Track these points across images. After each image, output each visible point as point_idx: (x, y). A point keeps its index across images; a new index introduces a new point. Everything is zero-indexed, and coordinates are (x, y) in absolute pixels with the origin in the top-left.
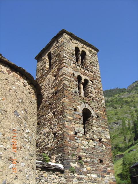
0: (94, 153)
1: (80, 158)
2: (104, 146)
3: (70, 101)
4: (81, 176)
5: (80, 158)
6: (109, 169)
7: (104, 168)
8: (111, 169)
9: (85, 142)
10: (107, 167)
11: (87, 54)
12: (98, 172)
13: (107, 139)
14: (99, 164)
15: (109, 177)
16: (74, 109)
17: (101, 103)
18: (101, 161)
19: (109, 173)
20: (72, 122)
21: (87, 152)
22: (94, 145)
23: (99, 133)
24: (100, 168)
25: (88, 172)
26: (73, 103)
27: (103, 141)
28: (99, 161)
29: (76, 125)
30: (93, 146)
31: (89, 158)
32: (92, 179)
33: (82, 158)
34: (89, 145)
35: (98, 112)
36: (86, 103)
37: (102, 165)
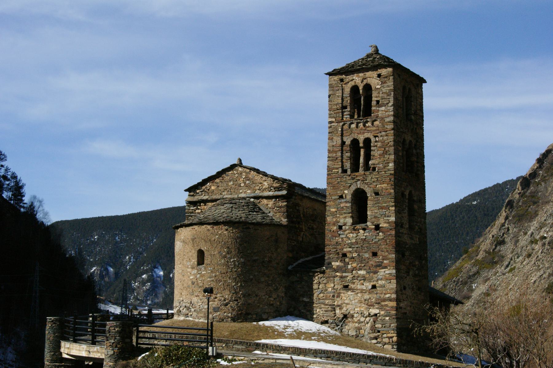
0: (363, 246)
1: (345, 255)
2: (381, 234)
3: (334, 188)
4: (344, 274)
5: (345, 255)
6: (385, 262)
7: (377, 262)
8: (390, 262)
9: (351, 235)
10: (383, 259)
11: (373, 89)
12: (368, 267)
13: (389, 223)
14: (371, 258)
15: (385, 272)
16: (338, 197)
17: (387, 170)
18: (375, 254)
19: (385, 267)
20: (335, 215)
21: (353, 246)
22: (366, 236)
23: (375, 217)
24: (371, 263)
25: (354, 269)
26: (338, 188)
27: (381, 227)
28: (371, 254)
29: (341, 216)
30: (364, 237)
31: (355, 253)
32: (358, 277)
33: (347, 254)
34: (357, 237)
35: (378, 186)
36: (359, 180)
37: (375, 259)
